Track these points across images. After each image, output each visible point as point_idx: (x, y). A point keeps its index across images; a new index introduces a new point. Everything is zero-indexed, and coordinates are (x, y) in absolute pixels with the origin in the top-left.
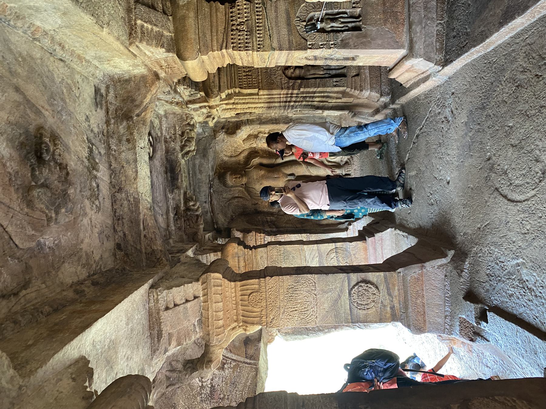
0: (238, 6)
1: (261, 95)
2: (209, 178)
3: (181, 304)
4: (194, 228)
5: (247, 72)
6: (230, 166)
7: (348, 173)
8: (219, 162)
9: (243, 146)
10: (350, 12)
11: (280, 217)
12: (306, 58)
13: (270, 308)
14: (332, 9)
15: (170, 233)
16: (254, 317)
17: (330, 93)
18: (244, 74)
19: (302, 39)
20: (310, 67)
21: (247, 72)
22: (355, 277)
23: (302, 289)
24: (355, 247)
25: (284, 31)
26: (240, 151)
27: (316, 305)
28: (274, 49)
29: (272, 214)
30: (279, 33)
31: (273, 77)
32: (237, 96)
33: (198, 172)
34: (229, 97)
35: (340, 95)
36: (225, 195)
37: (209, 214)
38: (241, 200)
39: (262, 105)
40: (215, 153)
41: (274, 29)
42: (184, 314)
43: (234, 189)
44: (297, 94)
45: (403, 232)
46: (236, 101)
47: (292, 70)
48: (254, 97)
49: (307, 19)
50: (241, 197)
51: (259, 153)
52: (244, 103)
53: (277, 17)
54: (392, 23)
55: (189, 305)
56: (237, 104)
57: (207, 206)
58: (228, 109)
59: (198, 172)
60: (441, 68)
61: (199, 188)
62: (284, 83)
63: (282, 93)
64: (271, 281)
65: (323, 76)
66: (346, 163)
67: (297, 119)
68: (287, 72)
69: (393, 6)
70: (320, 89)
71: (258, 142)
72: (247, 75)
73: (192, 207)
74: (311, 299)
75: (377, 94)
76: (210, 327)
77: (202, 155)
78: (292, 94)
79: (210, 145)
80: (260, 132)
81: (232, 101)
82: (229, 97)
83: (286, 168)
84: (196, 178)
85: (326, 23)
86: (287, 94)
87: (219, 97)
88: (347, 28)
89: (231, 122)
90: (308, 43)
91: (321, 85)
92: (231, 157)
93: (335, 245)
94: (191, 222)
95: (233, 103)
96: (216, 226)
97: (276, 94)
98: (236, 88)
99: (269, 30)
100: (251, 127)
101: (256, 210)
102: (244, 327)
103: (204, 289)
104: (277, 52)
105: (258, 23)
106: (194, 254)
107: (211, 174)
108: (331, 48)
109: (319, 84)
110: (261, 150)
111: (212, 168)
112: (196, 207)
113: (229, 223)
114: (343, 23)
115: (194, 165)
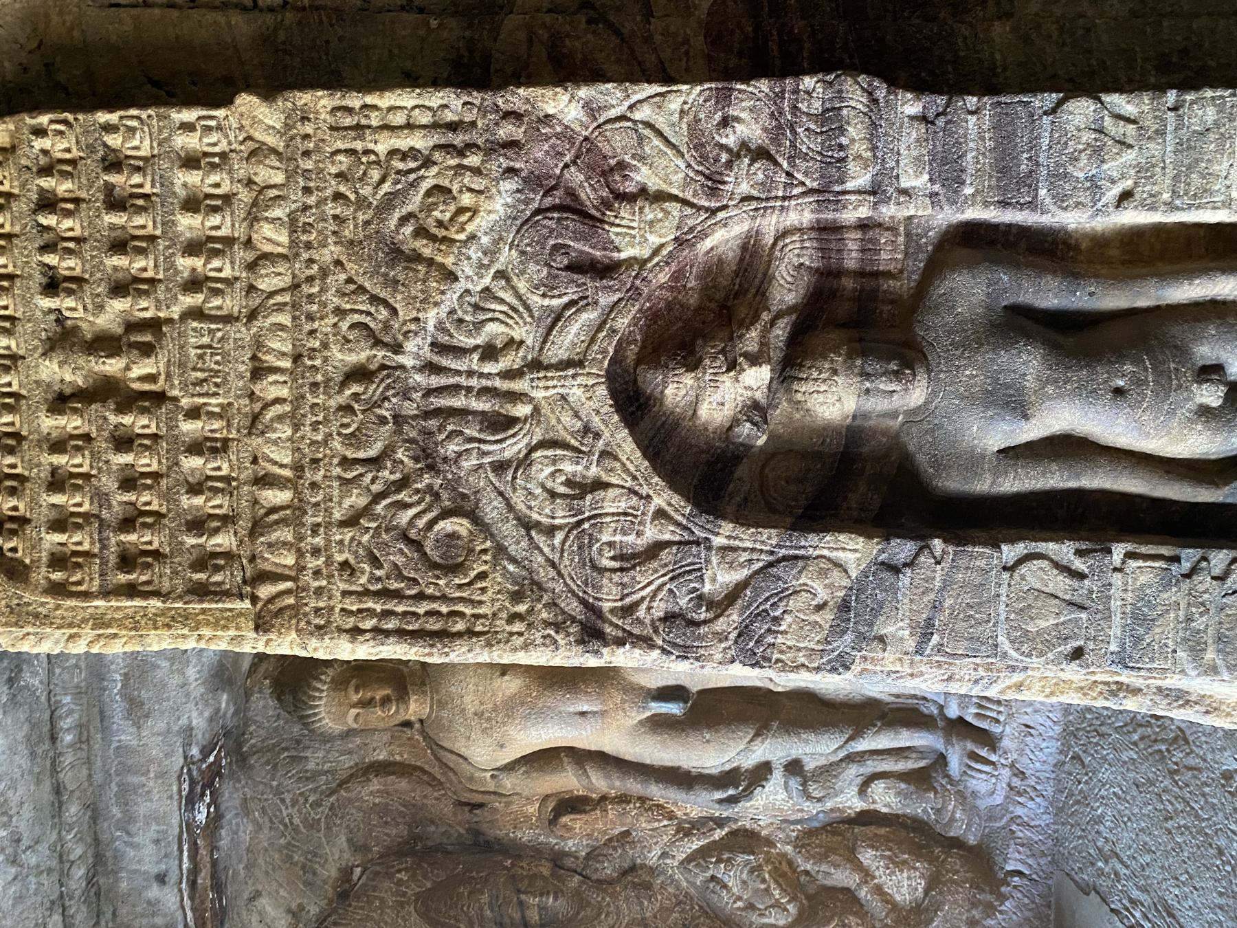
2: (187, 745)
11: (595, 897)
20: (1027, 364)
21: (105, 344)
29: (557, 859)
31: (469, 457)
33: (117, 708)
38: (403, 784)
57: (170, 899)
59: (117, 708)
61: (124, 803)
62: (630, 560)
68: (676, 390)
84: (106, 741)
101: (477, 833)
109: (1140, 619)
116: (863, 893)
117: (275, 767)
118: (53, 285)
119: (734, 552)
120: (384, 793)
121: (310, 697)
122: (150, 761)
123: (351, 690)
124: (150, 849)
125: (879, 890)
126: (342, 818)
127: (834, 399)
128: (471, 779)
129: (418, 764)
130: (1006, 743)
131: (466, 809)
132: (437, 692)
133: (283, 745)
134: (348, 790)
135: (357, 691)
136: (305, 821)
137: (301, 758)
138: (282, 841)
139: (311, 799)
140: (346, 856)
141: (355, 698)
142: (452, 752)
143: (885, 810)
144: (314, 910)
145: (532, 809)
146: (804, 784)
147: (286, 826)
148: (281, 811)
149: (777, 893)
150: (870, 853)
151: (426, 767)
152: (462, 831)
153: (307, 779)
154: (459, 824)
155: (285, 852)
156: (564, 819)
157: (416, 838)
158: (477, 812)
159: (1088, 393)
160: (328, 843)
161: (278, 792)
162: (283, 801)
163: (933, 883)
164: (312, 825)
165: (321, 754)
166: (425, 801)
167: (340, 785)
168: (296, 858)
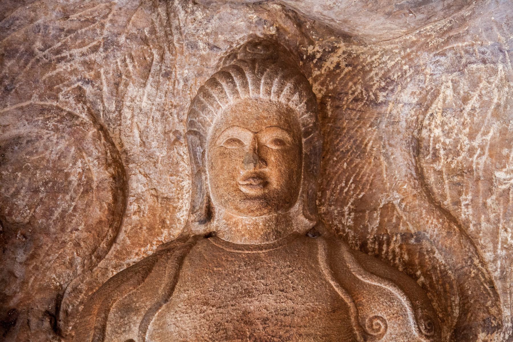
6: (346, 145)
26: (465, 213)
36: (142, 97)
38: (98, 213)
43: (185, 167)
50: (118, 213)
92: (417, 147)
117: (145, 41)
120: (87, 188)
121: (271, 78)
123: (279, 134)
126: (56, 130)
128: (127, 309)
129: (122, 236)
131: (51, 307)
132: (270, 254)
133: (168, 55)
134: (96, 138)
135: (278, 141)
136: (60, 79)
137: (146, 78)
138: (38, 44)
139: (88, 89)
141: (267, 138)
142: (176, 278)
147: (58, 51)
148: (80, 46)
151: (116, 247)
152: (12, 303)
153: (117, 85)
154: (28, 296)
155: (22, 48)
158: (47, 324)
160: (22, 108)
161: (109, 44)
162: (95, 49)
164: (52, 88)
166: (70, 245)
167: (102, 128)
168: (9, 63)
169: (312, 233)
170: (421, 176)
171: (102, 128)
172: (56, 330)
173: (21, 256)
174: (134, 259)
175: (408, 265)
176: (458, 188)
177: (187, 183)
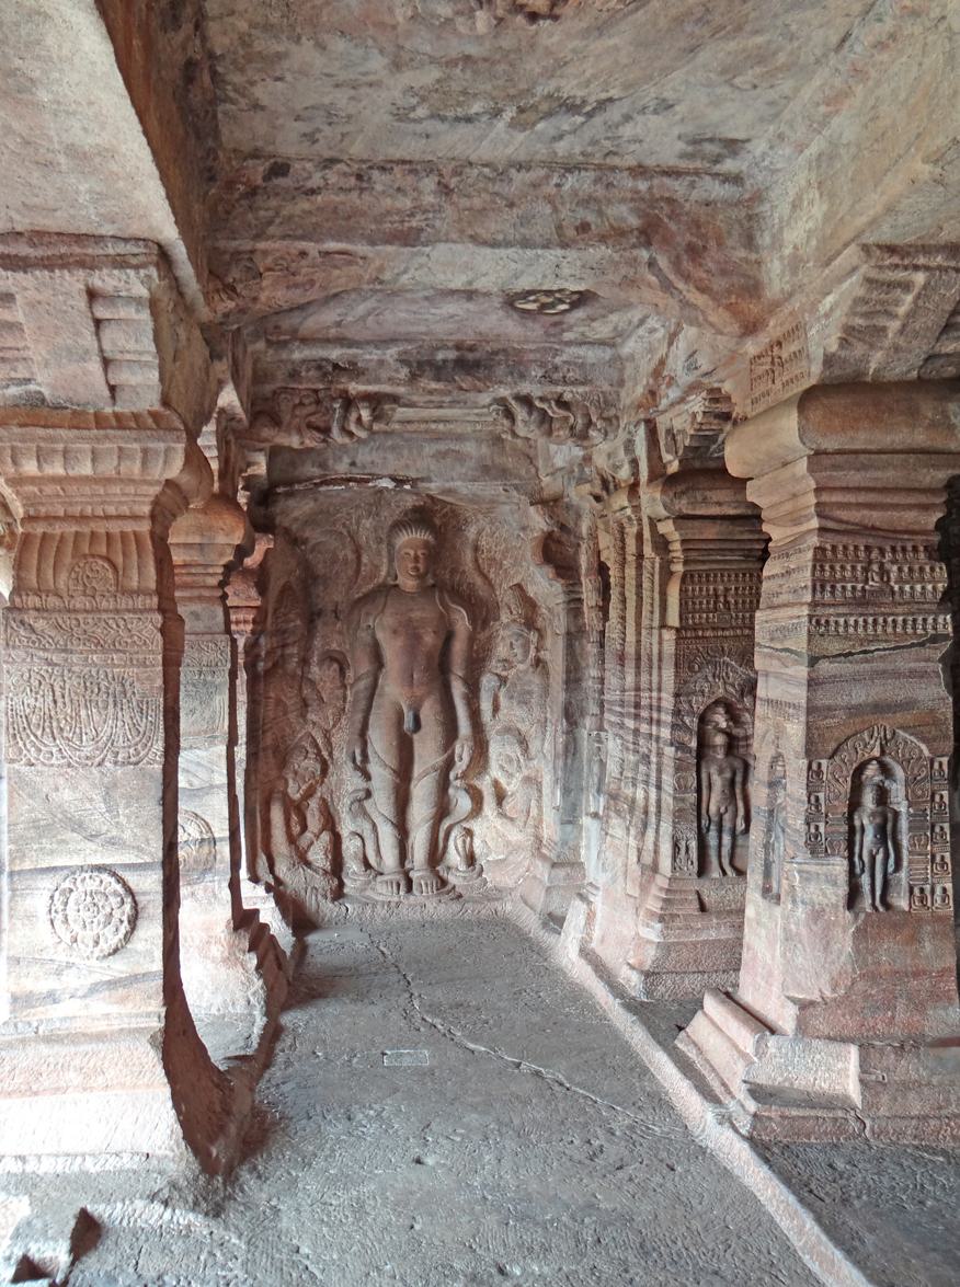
0: (932, 569)
1: (660, 636)
3: (99, 340)
4: (294, 416)
5: (725, 596)
7: (414, 887)
8: (468, 510)
9: (505, 586)
10: (900, 880)
12: (777, 758)
13: (66, 620)
14: (910, 829)
15: (283, 344)
16: (38, 570)
17: (657, 831)
18: (721, 587)
19: (833, 745)
20: (728, 775)
21: (725, 596)
22: (150, 884)
23: (120, 723)
24: (215, 895)
25: (859, 695)
26: (492, 576)
27: (69, 765)
28: (813, 661)
29: (305, 662)
30: (855, 679)
31: (708, 671)
32: (661, 568)
33: (442, 447)
34: (662, 544)
35: (648, 859)
36: (367, 523)
37: (316, 471)
38: (350, 572)
39: (631, 637)
40: (492, 502)
41: (867, 666)
42: (69, 351)
43: (384, 553)
44: (658, 739)
45: (262, 1037)
46: (647, 564)
47: (724, 725)
48: (657, 615)
49: (887, 759)
50: (358, 571)
51: (483, 629)
52: (639, 586)
53: (897, 675)
54: (867, 996)
55: (95, 366)
56: (639, 567)
57: (342, 468)
58: (623, 540)
59: (442, 447)
60: (743, 1132)
61: (393, 448)
62: (690, 702)
63: (664, 695)
64: (148, 628)
65: (704, 811)
66: (443, 883)
67: (575, 739)
69: (909, 999)
70: (668, 801)
71: (515, 628)
72: (717, 596)
73: (353, 416)
74: (88, 749)
75: (649, 962)
76: (16, 430)
77: (489, 463)
78: (659, 722)
79: (516, 488)
80: (541, 637)
81: (648, 550)
82: (662, 544)
83: (438, 707)
84: (425, 440)
85: (873, 814)
86: (659, 709)
87: (664, 513)
88: (858, 871)
89: (577, 553)
90: (824, 762)
91: (681, 805)
92: (476, 549)
93: (222, 839)
94: (312, 408)
95: (640, 556)
96: (280, 490)
97: (660, 676)
98: (686, 563)
99: (865, 652)
100: (561, 610)
101: (320, 614)
102: (7, 539)
103: (136, 417)
104: (802, 671)
105: (885, 621)
106: (222, 411)
107: (434, 487)
108: (808, 824)
109: (683, 800)
110: (490, 638)
111: (449, 491)
112: (353, 427)
113: (287, 531)
114: (873, 859)
115: (460, 438)
116: (308, 835)
118: (736, 589)
119: (691, 722)
120: (346, 562)
122: (415, 461)
124: (369, 459)
125: (312, 843)
127: (719, 740)
128: (368, 614)
130: (412, 898)
140: (313, 542)
141: (419, 553)
143: (344, 847)
144: (294, 527)
145: (334, 646)
146: (360, 801)
149: (304, 787)
150: (327, 838)
156: (335, 666)
157: (315, 578)
159: (723, 786)
161: (358, 507)
163: (326, 872)
164: (334, 524)
165: (368, 525)
167: (352, 538)
169: (434, 586)
170: (476, 560)
171: (352, 538)
172: (337, 617)
173: (321, 588)
174: (364, 590)
175: (469, 597)
176: (490, 566)
177: (385, 560)
